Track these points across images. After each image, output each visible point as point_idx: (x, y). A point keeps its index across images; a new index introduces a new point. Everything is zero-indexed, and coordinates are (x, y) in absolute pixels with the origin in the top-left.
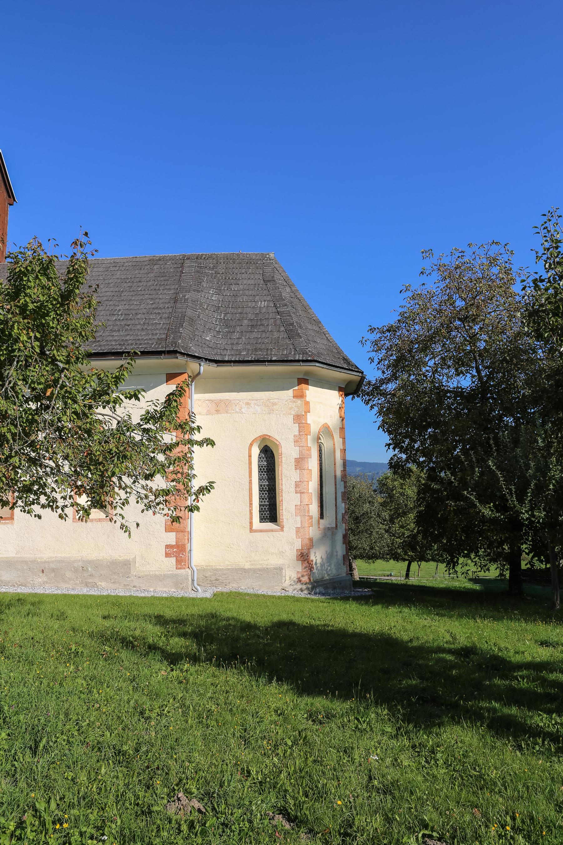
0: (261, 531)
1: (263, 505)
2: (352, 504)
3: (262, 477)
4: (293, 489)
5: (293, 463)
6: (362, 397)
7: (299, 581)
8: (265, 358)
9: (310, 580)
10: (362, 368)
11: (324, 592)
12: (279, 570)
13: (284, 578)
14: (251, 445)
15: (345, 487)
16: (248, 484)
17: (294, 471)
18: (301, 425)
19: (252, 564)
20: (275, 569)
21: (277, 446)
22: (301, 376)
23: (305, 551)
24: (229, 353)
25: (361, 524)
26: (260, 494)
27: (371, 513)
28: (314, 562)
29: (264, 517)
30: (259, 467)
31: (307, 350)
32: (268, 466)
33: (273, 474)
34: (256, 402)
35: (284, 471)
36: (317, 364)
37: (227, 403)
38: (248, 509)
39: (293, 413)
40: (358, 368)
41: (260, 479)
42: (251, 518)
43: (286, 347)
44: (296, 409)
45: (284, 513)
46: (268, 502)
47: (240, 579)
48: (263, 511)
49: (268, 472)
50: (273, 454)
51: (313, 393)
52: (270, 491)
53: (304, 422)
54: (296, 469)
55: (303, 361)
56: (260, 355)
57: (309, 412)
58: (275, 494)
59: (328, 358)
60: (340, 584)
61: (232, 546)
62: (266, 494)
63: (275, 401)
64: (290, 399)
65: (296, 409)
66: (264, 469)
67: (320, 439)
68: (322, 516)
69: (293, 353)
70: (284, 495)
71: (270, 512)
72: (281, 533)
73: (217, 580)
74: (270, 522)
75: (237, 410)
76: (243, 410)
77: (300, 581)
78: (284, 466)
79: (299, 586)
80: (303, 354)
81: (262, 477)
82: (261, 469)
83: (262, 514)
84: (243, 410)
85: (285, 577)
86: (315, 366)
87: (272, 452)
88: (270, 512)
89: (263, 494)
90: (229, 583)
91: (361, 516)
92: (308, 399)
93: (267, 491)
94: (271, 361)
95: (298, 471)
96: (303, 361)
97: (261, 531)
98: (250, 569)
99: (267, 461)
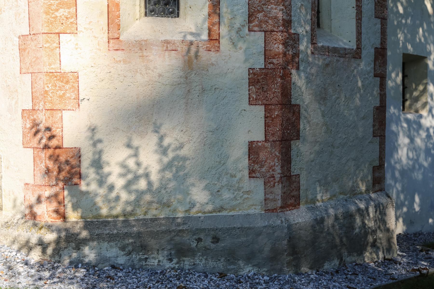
9: (64, 217)
77: (34, 216)
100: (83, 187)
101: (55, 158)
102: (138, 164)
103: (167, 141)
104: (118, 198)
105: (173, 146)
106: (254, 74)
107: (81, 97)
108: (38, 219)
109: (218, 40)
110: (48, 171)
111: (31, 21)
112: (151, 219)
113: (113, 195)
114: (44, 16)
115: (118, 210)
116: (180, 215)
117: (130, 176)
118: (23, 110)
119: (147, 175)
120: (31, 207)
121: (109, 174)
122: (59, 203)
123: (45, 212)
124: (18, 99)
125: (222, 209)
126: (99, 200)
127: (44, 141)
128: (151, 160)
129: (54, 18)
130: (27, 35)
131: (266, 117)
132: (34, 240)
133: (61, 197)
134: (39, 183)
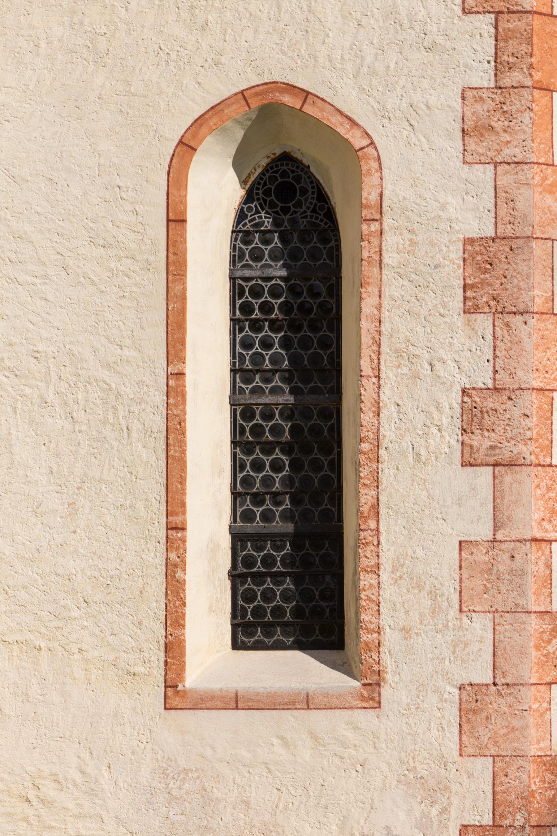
0: (237, 702)
1: (258, 539)
3: (257, 359)
4: (450, 440)
5: (453, 272)
14: (186, 147)
16: (159, 398)
17: (459, 320)
18: (511, 23)
21: (352, 158)
26: (237, 466)
29: (258, 612)
30: (237, 291)
32: (293, 291)
33: (325, 344)
35: (396, 324)
38: (156, 558)
42: (174, 617)
45: (388, 593)
46: (286, 516)
48: (258, 578)
49: (294, 327)
50: (330, 215)
52: (307, 449)
54: (471, 309)
58: (337, 466)
61: (50, 790)
62: (277, 467)
66: (266, 308)
72: (366, 718)
78: (394, 287)
81: (257, 359)
82: (246, 309)
83: (249, 597)
87: (322, 197)
89: (258, 466)
93: (287, 449)
95: (484, 322)
97: (237, 702)
99: (291, 257)
111: (499, 659)
114: (534, 653)
118: (465, 827)
124: (450, 804)
129: (545, 656)
130: (487, 685)
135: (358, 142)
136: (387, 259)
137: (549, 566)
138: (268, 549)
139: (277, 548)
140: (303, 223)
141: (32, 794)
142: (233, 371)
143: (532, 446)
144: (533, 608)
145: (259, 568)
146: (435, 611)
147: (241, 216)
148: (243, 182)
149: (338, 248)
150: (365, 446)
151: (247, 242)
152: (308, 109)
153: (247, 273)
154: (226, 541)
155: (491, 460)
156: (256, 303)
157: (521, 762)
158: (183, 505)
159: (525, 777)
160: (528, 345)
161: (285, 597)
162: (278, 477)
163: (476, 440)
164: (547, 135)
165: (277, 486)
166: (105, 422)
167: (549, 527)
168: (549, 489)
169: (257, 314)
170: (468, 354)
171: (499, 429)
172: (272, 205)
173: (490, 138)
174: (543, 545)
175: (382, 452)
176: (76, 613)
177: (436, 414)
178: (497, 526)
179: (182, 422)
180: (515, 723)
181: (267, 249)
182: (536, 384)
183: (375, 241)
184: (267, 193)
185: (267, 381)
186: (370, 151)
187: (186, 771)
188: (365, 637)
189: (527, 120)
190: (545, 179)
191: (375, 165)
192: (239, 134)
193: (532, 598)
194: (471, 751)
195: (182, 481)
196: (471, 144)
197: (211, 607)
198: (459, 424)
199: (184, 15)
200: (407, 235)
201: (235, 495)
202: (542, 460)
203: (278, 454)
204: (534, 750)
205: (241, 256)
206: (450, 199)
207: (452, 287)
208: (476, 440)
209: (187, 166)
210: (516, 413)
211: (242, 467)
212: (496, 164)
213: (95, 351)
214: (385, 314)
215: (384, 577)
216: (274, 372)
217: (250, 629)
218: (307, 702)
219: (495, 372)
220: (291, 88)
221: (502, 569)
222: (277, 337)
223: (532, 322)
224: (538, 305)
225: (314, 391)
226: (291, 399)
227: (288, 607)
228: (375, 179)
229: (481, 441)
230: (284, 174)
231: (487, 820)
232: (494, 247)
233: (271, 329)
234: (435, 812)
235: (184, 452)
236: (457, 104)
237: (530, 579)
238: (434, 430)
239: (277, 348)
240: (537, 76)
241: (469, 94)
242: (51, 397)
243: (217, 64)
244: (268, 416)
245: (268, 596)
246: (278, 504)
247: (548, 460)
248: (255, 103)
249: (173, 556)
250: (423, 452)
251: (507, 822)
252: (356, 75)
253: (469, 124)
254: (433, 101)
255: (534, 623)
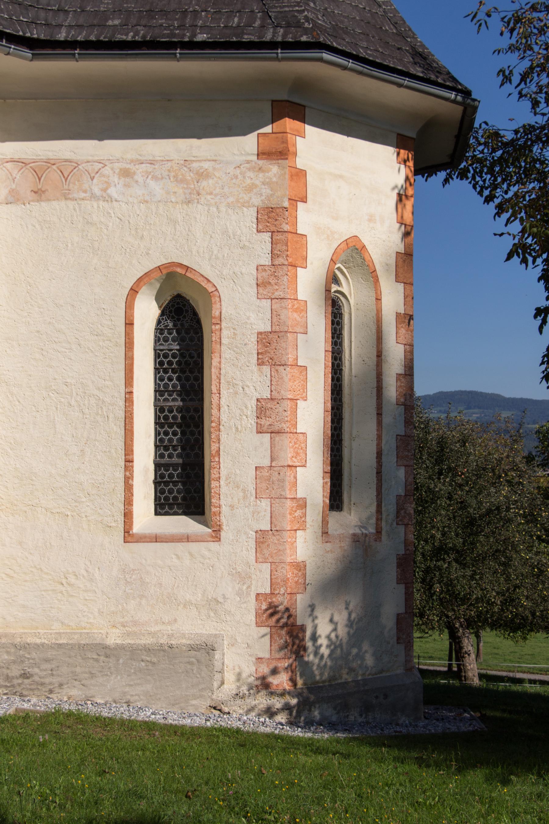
0: (156, 539)
1: (166, 466)
2: (460, 486)
4: (251, 422)
5: (253, 347)
6: (474, 178)
7: (264, 685)
8: (174, 35)
9: (295, 684)
10: (466, 81)
11: (334, 719)
12: (206, 650)
13: (218, 676)
14: (134, 291)
15: (408, 422)
16: (122, 403)
17: (255, 368)
18: (279, 237)
19: (129, 634)
20: (192, 648)
21: (208, 296)
22: (284, 96)
23: (280, 599)
24: (70, 20)
25: (482, 538)
26: (157, 433)
27: (508, 509)
28: (308, 634)
29: (166, 499)
30: (157, 355)
31: (301, 17)
32: (182, 355)
34: (149, 168)
36: (326, 56)
37: (68, 170)
38: (120, 475)
39: (257, 201)
40: (454, 79)
41: (158, 391)
42: (128, 501)
43: (239, 6)
44: (266, 191)
45: (224, 490)
46: (179, 456)
47: (92, 675)
48: (166, 483)
49: (183, 371)
51: (316, 147)
53: (286, 227)
54: (260, 363)
55: (286, 45)
56: (164, 28)
57: (304, 200)
58: (201, 433)
59: (365, 44)
60: (386, 696)
61: (72, 580)
62: (175, 434)
63: (206, 165)
64: (248, 162)
65: (266, 191)
66: (170, 363)
67: (336, 280)
68: (336, 501)
69: (257, 23)
70: (223, 437)
71: (184, 485)
72: (213, 546)
73: (25, 676)
74: (185, 514)
75: (97, 191)
76: (112, 191)
78: (227, 353)
79: (262, 701)
80: (288, 25)
82: (161, 363)
84: (112, 191)
85: (221, 672)
86: (321, 60)
87: (195, 314)
88: (184, 485)
89: (166, 433)
90: (61, 685)
91: (481, 517)
92: (300, 163)
93: (179, 426)
94: (192, 45)
95: (266, 369)
96: (286, 45)
97: (156, 539)
98: (122, 648)
99: (181, 340)
100: (306, 659)
101: (290, 633)
102: (337, 637)
103: (353, 616)
104: (325, 665)
105: (356, 620)
106: (399, 559)
107: (307, 582)
108: (274, 687)
109: (380, 532)
110: (285, 646)
111: (274, 519)
112: (345, 683)
113: (323, 663)
114: (289, 516)
115: (326, 676)
116: (360, 678)
117: (332, 647)
118: (258, 594)
119: (341, 645)
120: (264, 678)
121: (321, 646)
122: (292, 672)
123: (282, 681)
124: (251, 584)
125: (381, 671)
126: (315, 668)
127: (284, 620)
128: (342, 631)
129: (294, 517)
130: (268, 531)
131: (406, 593)
132: (278, 705)
133: (294, 667)
134: (278, 656)
135: (210, 289)
136: (223, 341)
137: (295, 478)
138: (171, 471)
139: (175, 470)
140: (186, 325)
141: (64, 581)
142: (156, 391)
143: (288, 424)
144: (288, 496)
145: (167, 479)
146: (245, 498)
147: (159, 322)
148: (160, 307)
149: (202, 336)
150: (213, 425)
151: (161, 334)
152: (188, 274)
153: (162, 348)
154: (152, 467)
155: (270, 431)
156: (166, 361)
157: (283, 565)
158: (132, 451)
159: (285, 572)
160: (286, 379)
161: (179, 492)
162: (175, 438)
163: (263, 422)
164: (295, 286)
165: (175, 442)
166: (97, 414)
167: (295, 460)
168: (295, 443)
169: (166, 366)
170: (259, 383)
171: (273, 417)
172: (173, 317)
173: (269, 288)
174: (293, 468)
175: (221, 427)
176: (84, 499)
177: (245, 410)
178: (272, 460)
179: (132, 414)
180: (281, 548)
181: (170, 337)
182: (290, 397)
183: (218, 333)
184: (171, 312)
185: (170, 395)
186: (216, 293)
187: (133, 570)
188: (213, 510)
189: (285, 280)
190: (293, 306)
191: (218, 299)
192: (158, 286)
193: (288, 492)
194: (261, 560)
195: (132, 440)
196: (261, 290)
197: (145, 497)
198: (255, 414)
199: (133, 232)
200: (232, 331)
201: (156, 446)
202: (292, 430)
203: (175, 428)
204: (289, 560)
205: (159, 340)
206: (251, 315)
207: (252, 353)
208: (263, 422)
209: (134, 300)
210: (281, 409)
211: (159, 434)
212: (272, 299)
213: (93, 382)
214: (223, 366)
215: (222, 482)
216: (173, 391)
217: (162, 507)
218: (187, 539)
219: (271, 391)
220: (181, 265)
221: (275, 479)
222: (175, 376)
223: (288, 369)
224: (290, 361)
225: (191, 400)
226: (181, 404)
227: (180, 496)
228: (218, 306)
229: (265, 422)
230: (178, 303)
231: (268, 591)
232: (271, 336)
233: (173, 372)
234: (245, 587)
235: (132, 427)
236: (254, 272)
237: (287, 484)
238: (244, 417)
239: (175, 381)
240: (290, 260)
241: (260, 268)
242: (73, 403)
243: (148, 254)
244: (171, 411)
245: (171, 491)
246: (175, 450)
247: (295, 431)
248: (165, 272)
249: (128, 474)
250: (239, 427)
251: (277, 592)
252: (210, 260)
253: (260, 281)
254: (244, 271)
255: (289, 503)
